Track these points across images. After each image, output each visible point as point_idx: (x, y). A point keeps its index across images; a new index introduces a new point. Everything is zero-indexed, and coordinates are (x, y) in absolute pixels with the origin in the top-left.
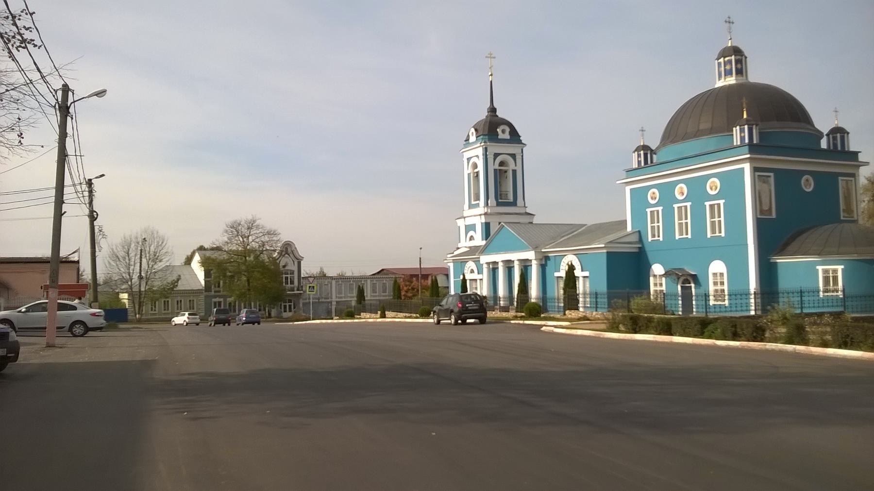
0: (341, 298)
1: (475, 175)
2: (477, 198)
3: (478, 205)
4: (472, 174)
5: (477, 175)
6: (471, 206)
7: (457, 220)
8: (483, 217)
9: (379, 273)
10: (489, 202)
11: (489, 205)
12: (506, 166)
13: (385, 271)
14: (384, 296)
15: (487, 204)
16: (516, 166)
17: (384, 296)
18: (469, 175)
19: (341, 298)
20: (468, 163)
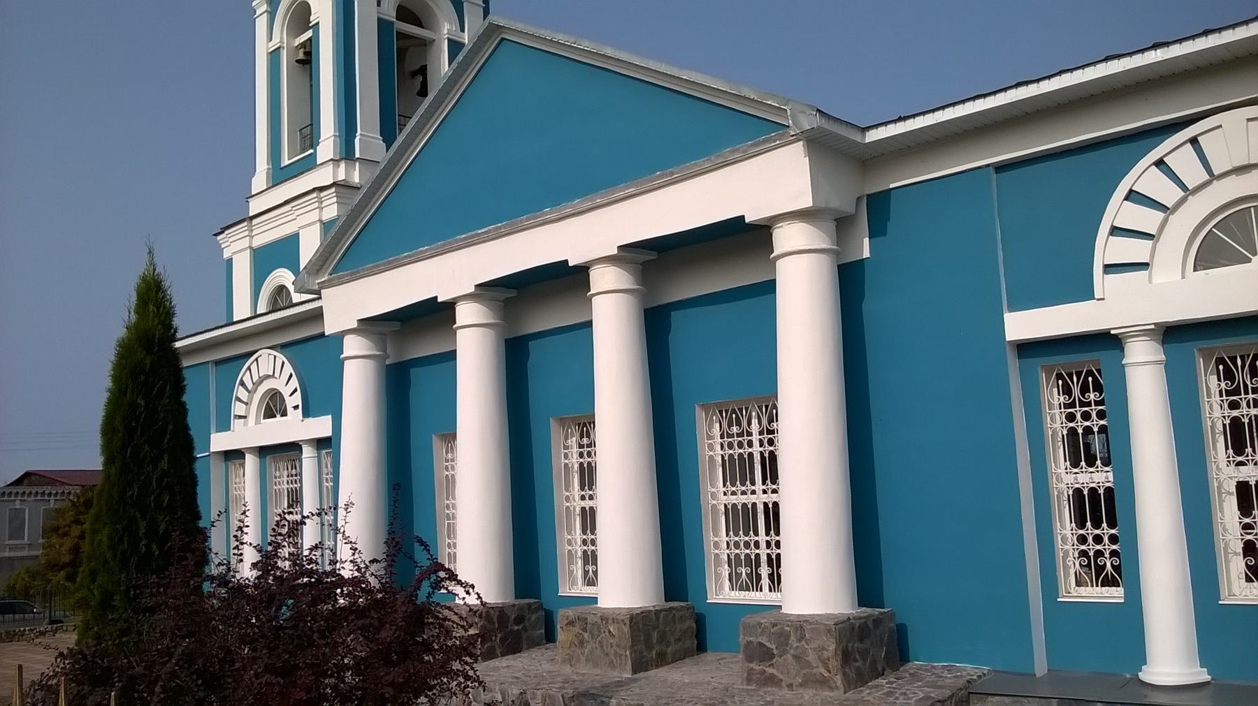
0: (22, 547)
1: (301, 56)
2: (309, 137)
3: (309, 164)
4: (284, 54)
5: (307, 59)
6: (280, 176)
7: (219, 238)
8: (330, 198)
9: (18, 482)
10: (357, 141)
11: (357, 155)
12: (419, 24)
13: (33, 478)
14: (12, 548)
15: (346, 153)
16: (463, 30)
17: (12, 548)
18: (274, 55)
19: (22, 547)
20: (272, 15)
